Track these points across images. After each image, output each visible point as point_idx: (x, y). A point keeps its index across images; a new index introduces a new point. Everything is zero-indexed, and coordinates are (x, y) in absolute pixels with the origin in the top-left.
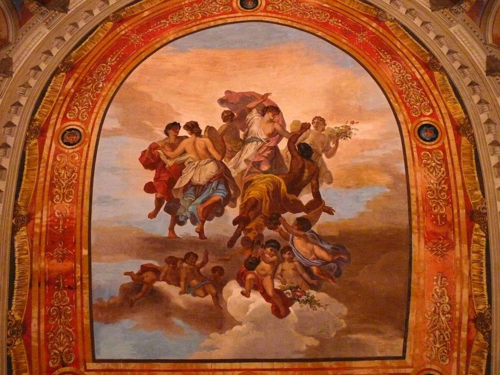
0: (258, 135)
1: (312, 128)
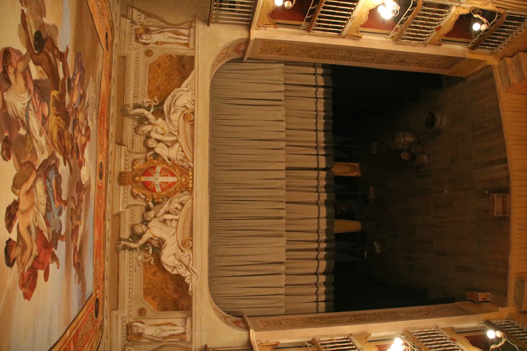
0: (24, 104)
1: (25, 10)
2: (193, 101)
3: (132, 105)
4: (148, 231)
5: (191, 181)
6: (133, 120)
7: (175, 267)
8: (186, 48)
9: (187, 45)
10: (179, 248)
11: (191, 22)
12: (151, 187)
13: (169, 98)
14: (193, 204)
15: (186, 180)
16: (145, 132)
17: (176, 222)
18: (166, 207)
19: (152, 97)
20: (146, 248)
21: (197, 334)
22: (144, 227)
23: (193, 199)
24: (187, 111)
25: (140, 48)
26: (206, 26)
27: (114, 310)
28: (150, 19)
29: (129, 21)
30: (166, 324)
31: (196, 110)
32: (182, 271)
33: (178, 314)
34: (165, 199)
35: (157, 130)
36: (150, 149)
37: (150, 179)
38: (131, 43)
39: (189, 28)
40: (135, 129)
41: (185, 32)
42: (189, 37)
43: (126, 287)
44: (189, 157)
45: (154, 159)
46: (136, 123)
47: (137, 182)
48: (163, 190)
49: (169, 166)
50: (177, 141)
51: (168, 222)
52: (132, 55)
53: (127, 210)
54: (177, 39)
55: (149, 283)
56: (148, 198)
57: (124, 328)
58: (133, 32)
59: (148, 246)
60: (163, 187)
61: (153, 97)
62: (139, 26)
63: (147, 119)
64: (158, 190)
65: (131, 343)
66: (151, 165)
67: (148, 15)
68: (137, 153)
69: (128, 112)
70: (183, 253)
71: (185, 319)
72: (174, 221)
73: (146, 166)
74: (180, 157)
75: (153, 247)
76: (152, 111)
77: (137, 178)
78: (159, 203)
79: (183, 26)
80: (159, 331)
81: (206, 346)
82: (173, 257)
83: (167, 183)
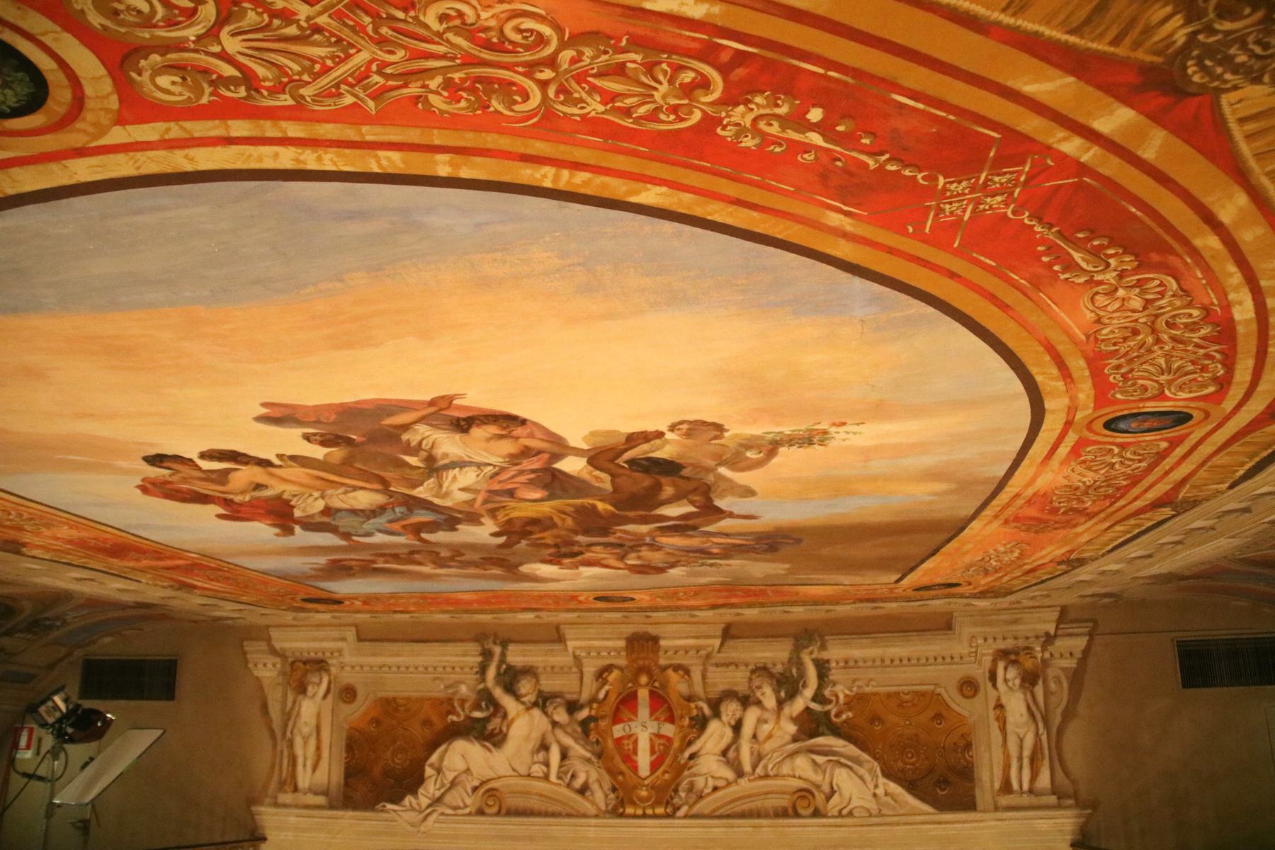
2: (850, 814)
3: (825, 655)
4: (521, 707)
5: (640, 812)
6: (786, 661)
7: (439, 770)
8: (997, 785)
9: (1006, 788)
10: (483, 783)
11: (1075, 796)
12: (625, 713)
13: (852, 750)
14: (585, 816)
15: (642, 800)
16: (758, 694)
17: (541, 774)
18: (578, 750)
19: (849, 704)
20: (483, 704)
21: (292, 818)
22: (530, 698)
23: (596, 816)
24: (820, 798)
25: (980, 664)
26: (1069, 837)
27: (358, 632)
28: (1065, 685)
29: (1051, 628)
30: (318, 748)
31: (824, 821)
32: (430, 788)
33: (337, 776)
34: (597, 749)
35: (766, 722)
36: (715, 706)
37: (644, 711)
38: (990, 641)
39: (1054, 791)
40: (765, 668)
41: (1044, 780)
42: (1031, 791)
43: (401, 659)
44: (700, 807)
45: (691, 719)
46: (779, 668)
47: (635, 680)
48: (618, 741)
49: (676, 757)
50: (740, 774)
51: (541, 756)
52: (957, 646)
53: (571, 658)
54: (1020, 758)
55: (407, 710)
56: (599, 707)
57: (320, 655)
58: (1021, 643)
59: (487, 708)
60: (626, 742)
61: (850, 709)
62: (1039, 655)
63: (792, 695)
64: (618, 731)
65: (288, 669)
66: (677, 713)
67: (1076, 678)
68: (704, 677)
69: (806, 647)
70: (470, 791)
71: (326, 793)
72: (545, 769)
73: (674, 699)
74: (700, 782)
75: (486, 720)
76: (814, 706)
77: (644, 679)
78: (586, 733)
79: (1060, 774)
80: (306, 730)
81: (264, 839)
82: (461, 766)
83: (635, 752)
